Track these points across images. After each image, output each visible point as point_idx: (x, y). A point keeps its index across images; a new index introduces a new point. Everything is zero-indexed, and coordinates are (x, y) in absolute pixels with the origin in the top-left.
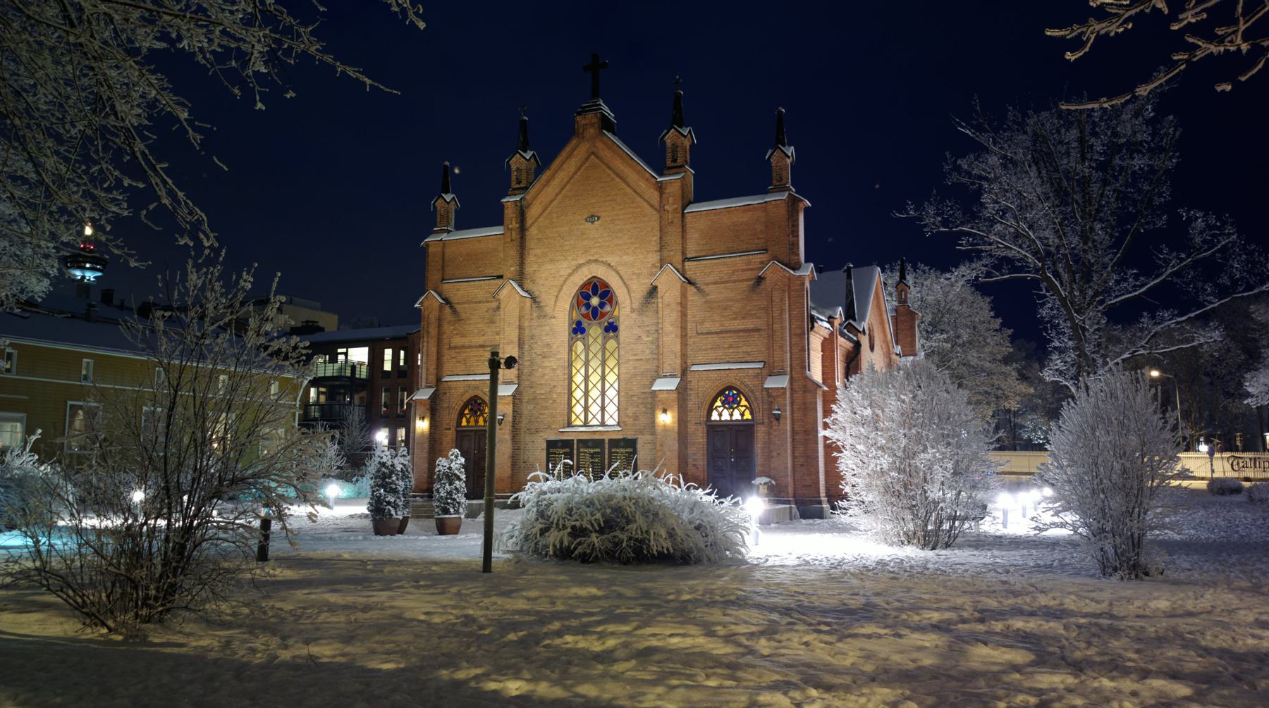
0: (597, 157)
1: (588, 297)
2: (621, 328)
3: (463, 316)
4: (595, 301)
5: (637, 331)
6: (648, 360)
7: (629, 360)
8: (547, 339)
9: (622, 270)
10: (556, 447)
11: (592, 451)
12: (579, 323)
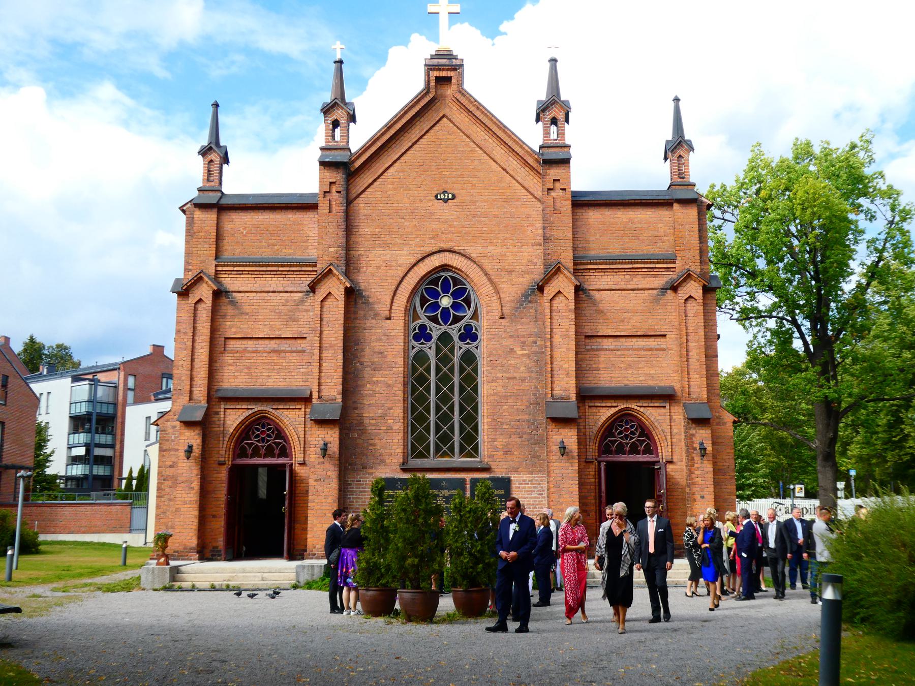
1: (436, 295)
2: (483, 335)
3: (247, 308)
4: (446, 302)
5: (508, 342)
6: (523, 380)
7: (497, 378)
8: (377, 346)
10: (394, 488)
11: (446, 493)
12: (423, 327)
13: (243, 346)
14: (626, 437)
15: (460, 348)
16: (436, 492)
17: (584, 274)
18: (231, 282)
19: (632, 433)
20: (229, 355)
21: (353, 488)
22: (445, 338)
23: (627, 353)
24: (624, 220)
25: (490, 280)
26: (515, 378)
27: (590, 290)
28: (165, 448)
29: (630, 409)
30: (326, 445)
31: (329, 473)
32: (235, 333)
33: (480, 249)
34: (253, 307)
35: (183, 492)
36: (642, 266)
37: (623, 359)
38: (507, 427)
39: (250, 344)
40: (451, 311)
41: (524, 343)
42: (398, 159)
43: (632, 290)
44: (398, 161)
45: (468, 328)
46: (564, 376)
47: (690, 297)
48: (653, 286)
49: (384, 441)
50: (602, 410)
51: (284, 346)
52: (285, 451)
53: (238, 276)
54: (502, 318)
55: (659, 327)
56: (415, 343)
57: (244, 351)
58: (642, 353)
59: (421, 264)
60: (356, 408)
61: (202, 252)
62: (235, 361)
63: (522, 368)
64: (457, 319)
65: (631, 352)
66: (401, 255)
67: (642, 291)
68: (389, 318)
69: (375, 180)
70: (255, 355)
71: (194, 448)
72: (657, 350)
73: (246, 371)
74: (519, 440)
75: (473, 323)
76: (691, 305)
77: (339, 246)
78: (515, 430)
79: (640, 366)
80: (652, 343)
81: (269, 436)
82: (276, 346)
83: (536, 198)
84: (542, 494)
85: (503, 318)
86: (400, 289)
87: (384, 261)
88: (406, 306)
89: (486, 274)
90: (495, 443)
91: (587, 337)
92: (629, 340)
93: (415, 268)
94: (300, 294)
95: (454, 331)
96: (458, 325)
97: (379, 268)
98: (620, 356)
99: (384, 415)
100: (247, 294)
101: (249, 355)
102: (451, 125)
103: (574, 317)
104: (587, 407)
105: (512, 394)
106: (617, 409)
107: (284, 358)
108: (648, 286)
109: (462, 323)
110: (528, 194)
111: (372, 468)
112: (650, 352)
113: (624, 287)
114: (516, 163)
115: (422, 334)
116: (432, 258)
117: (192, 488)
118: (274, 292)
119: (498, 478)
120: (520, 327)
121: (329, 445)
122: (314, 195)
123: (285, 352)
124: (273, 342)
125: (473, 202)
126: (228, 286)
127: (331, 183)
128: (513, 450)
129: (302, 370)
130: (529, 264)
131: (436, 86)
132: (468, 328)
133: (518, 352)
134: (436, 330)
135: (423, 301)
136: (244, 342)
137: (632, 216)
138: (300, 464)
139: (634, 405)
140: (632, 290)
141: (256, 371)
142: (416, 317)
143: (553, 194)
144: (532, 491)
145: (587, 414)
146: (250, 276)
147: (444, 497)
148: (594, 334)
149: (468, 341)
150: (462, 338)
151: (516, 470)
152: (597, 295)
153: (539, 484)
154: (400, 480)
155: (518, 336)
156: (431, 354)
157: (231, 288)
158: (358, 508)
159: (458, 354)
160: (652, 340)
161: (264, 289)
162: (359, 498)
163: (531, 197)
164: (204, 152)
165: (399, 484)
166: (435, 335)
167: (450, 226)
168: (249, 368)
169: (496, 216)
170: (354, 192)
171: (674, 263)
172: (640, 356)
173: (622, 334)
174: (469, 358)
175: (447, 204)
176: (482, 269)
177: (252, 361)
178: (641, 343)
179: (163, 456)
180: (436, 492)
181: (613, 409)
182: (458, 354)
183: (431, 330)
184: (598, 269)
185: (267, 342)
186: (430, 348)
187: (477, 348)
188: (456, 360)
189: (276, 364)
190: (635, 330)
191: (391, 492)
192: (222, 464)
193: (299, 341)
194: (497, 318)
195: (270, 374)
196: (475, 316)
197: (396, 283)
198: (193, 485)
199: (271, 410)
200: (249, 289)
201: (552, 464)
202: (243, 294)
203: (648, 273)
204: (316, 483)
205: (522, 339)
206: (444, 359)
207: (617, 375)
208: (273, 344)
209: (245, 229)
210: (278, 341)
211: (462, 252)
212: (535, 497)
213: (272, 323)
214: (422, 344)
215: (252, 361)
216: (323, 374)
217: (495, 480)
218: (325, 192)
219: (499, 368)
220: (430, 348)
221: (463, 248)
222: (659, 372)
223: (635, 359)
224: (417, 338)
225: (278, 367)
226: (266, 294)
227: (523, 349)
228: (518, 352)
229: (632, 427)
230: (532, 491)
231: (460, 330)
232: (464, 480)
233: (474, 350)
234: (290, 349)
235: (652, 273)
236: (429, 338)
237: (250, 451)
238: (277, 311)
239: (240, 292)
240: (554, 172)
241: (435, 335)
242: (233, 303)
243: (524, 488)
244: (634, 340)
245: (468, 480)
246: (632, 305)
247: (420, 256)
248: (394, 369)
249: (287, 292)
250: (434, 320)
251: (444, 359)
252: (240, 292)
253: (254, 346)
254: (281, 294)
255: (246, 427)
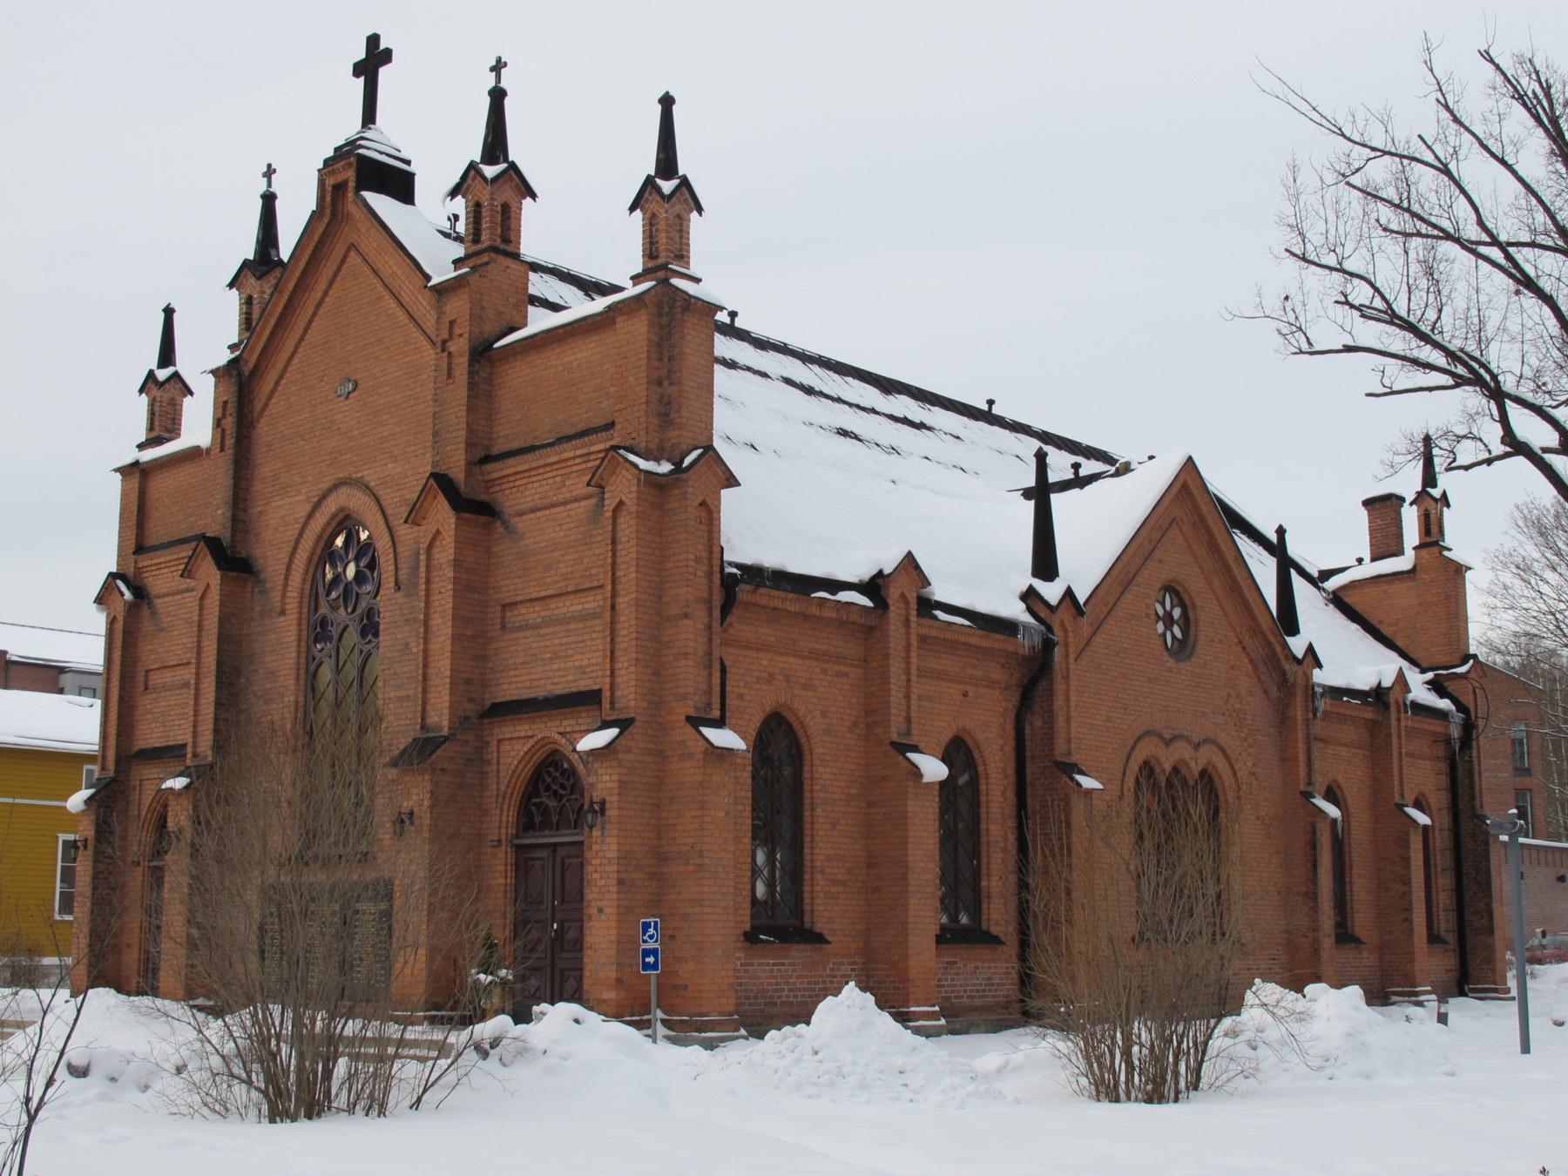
12: (324, 622)
36: (571, 454)
44: (303, 344)
45: (371, 613)
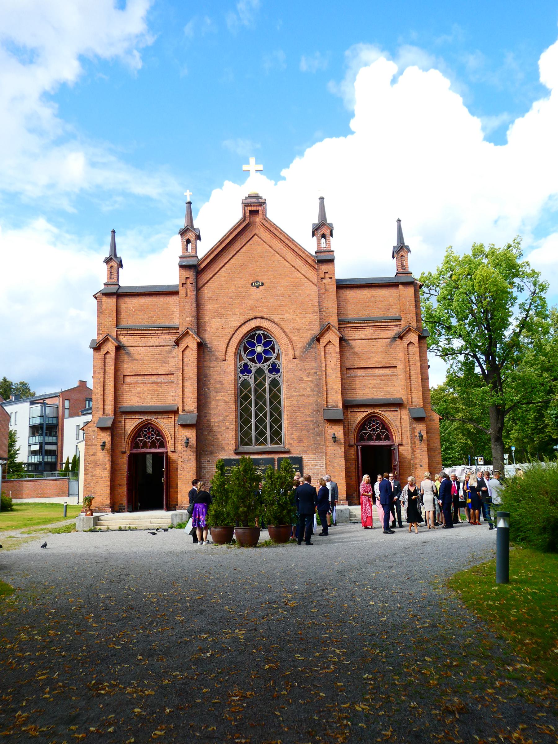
0: (257, 235)
1: (253, 345)
2: (283, 369)
3: (136, 357)
4: (259, 349)
6: (309, 396)
8: (218, 378)
9: (283, 324)
11: (263, 467)
12: (246, 365)
13: (135, 380)
14: (374, 430)
15: (269, 377)
16: (257, 467)
17: (345, 330)
18: (126, 341)
19: (377, 428)
20: (127, 385)
21: (205, 466)
22: (260, 371)
23: (372, 378)
24: (369, 296)
25: (286, 335)
26: (304, 395)
27: (349, 340)
28: (88, 444)
29: (376, 413)
30: (188, 440)
31: (190, 457)
32: (130, 372)
33: (280, 316)
34: (140, 356)
35: (100, 471)
36: (381, 324)
37: (370, 382)
38: (300, 425)
39: (139, 379)
40: (263, 355)
41: (309, 373)
42: (228, 262)
43: (374, 339)
44: (228, 263)
45: (274, 365)
46: (335, 393)
47: (411, 342)
48: (387, 337)
49: (224, 436)
50: (358, 414)
51: (161, 379)
52: (162, 444)
53: (131, 337)
54: (295, 358)
55: (392, 361)
56: (242, 375)
57: (136, 383)
58: (382, 378)
59: (243, 327)
60: (206, 416)
61: (108, 323)
62: (131, 389)
63: (308, 389)
64: (267, 360)
65: (375, 378)
66: (231, 321)
67: (381, 340)
68: (225, 360)
69: (213, 276)
70: (142, 385)
71: (106, 443)
72: (391, 376)
73: (137, 395)
74: (307, 434)
75: (277, 362)
76: (411, 347)
77: (192, 317)
78: (304, 427)
79: (381, 386)
80: (388, 371)
81: (152, 435)
82: (156, 379)
83: (314, 284)
84: (322, 467)
85: (295, 358)
86: (231, 342)
87: (221, 325)
88: (235, 352)
89: (284, 332)
90: (293, 436)
91: (348, 369)
92: (374, 370)
93: (240, 329)
94: (169, 347)
95: (265, 367)
96: (267, 363)
97: (217, 329)
98: (369, 380)
99: (223, 420)
100: (136, 348)
101: (139, 385)
102: (260, 240)
103: (339, 356)
104: (349, 412)
105: (302, 405)
106: (367, 413)
107: (161, 386)
108: (384, 337)
109: (270, 362)
110: (309, 281)
111: (216, 453)
112: (387, 377)
113: (370, 337)
114: (301, 262)
115: (246, 370)
116: (250, 322)
117: (106, 469)
118: (153, 346)
119: (295, 458)
120: (306, 363)
121: (190, 440)
122: (177, 286)
123: (161, 383)
124: (154, 377)
125: (275, 287)
126: (125, 343)
127: (186, 278)
128: (303, 440)
129: (172, 394)
130: (310, 324)
131: (249, 215)
132: (274, 365)
133: (305, 379)
134: (254, 367)
135: (246, 349)
136: (136, 377)
137: (373, 294)
138: (172, 452)
139: (378, 410)
140: (374, 339)
141: (144, 395)
142: (241, 359)
143: (324, 281)
144: (316, 465)
145: (349, 416)
146: (138, 337)
147: (261, 470)
148: (352, 367)
149: (274, 373)
150: (270, 371)
151: (306, 452)
152: (353, 343)
153: (320, 460)
154: (234, 459)
155: (305, 370)
156: (252, 381)
157: (126, 344)
158: (209, 478)
159: (268, 381)
160: (388, 369)
161: (147, 345)
162: (209, 472)
163: (311, 283)
164: (108, 261)
165: (234, 463)
166: (253, 370)
167: (261, 302)
168: (139, 393)
169: (289, 296)
170: (201, 283)
171: (400, 321)
172: (381, 380)
173: (369, 366)
174: (275, 384)
175: (259, 289)
176: (281, 328)
177: (141, 389)
178: (381, 371)
179: (88, 449)
180: (257, 467)
181: (365, 413)
182: (268, 381)
183: (251, 367)
184: (353, 327)
185: (150, 377)
186: (251, 378)
187: (280, 377)
188: (267, 385)
189: (155, 391)
190: (377, 364)
191: (229, 468)
192: (124, 453)
193: (170, 376)
194: (292, 358)
195: (152, 397)
196: (278, 358)
197: (229, 338)
198: (106, 467)
199: (153, 419)
200: (137, 345)
201: (328, 448)
202: (134, 348)
203: (385, 328)
204: (182, 463)
205: (307, 371)
206: (260, 385)
207: (367, 392)
208: (153, 378)
209: (134, 308)
210: (157, 377)
211: (269, 318)
212: (318, 469)
213: (152, 365)
214: (246, 375)
215: (141, 389)
216: (185, 396)
217: (292, 458)
218: (183, 284)
219: (294, 389)
220: (251, 378)
221: (269, 316)
222: (393, 389)
223: (378, 382)
224: (242, 372)
225: (157, 392)
226: (148, 348)
227: (308, 378)
228: (305, 379)
229: (377, 424)
230: (316, 465)
231: (269, 366)
232: (274, 459)
233: (278, 379)
234: (164, 381)
235: (386, 328)
236: (249, 372)
237: (141, 445)
238: (155, 358)
239: (132, 347)
240: (325, 268)
241: (253, 370)
242: (128, 353)
243: (311, 463)
244: (377, 370)
245: (276, 458)
246: (375, 348)
247: (243, 322)
248: (229, 392)
249: (161, 346)
250: (253, 360)
251: (260, 385)
252: (132, 347)
253: (142, 380)
254: (157, 348)
255: (139, 429)
